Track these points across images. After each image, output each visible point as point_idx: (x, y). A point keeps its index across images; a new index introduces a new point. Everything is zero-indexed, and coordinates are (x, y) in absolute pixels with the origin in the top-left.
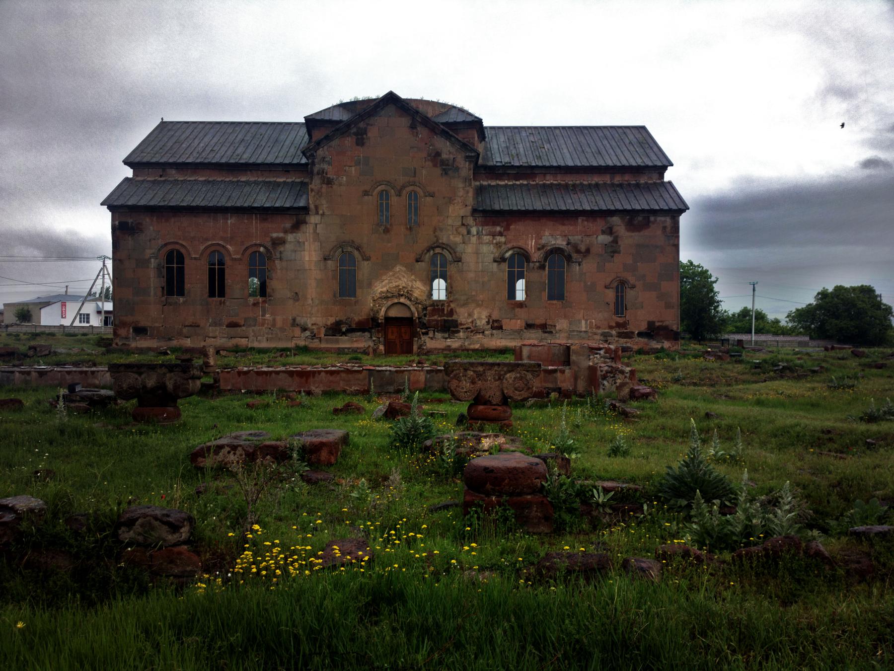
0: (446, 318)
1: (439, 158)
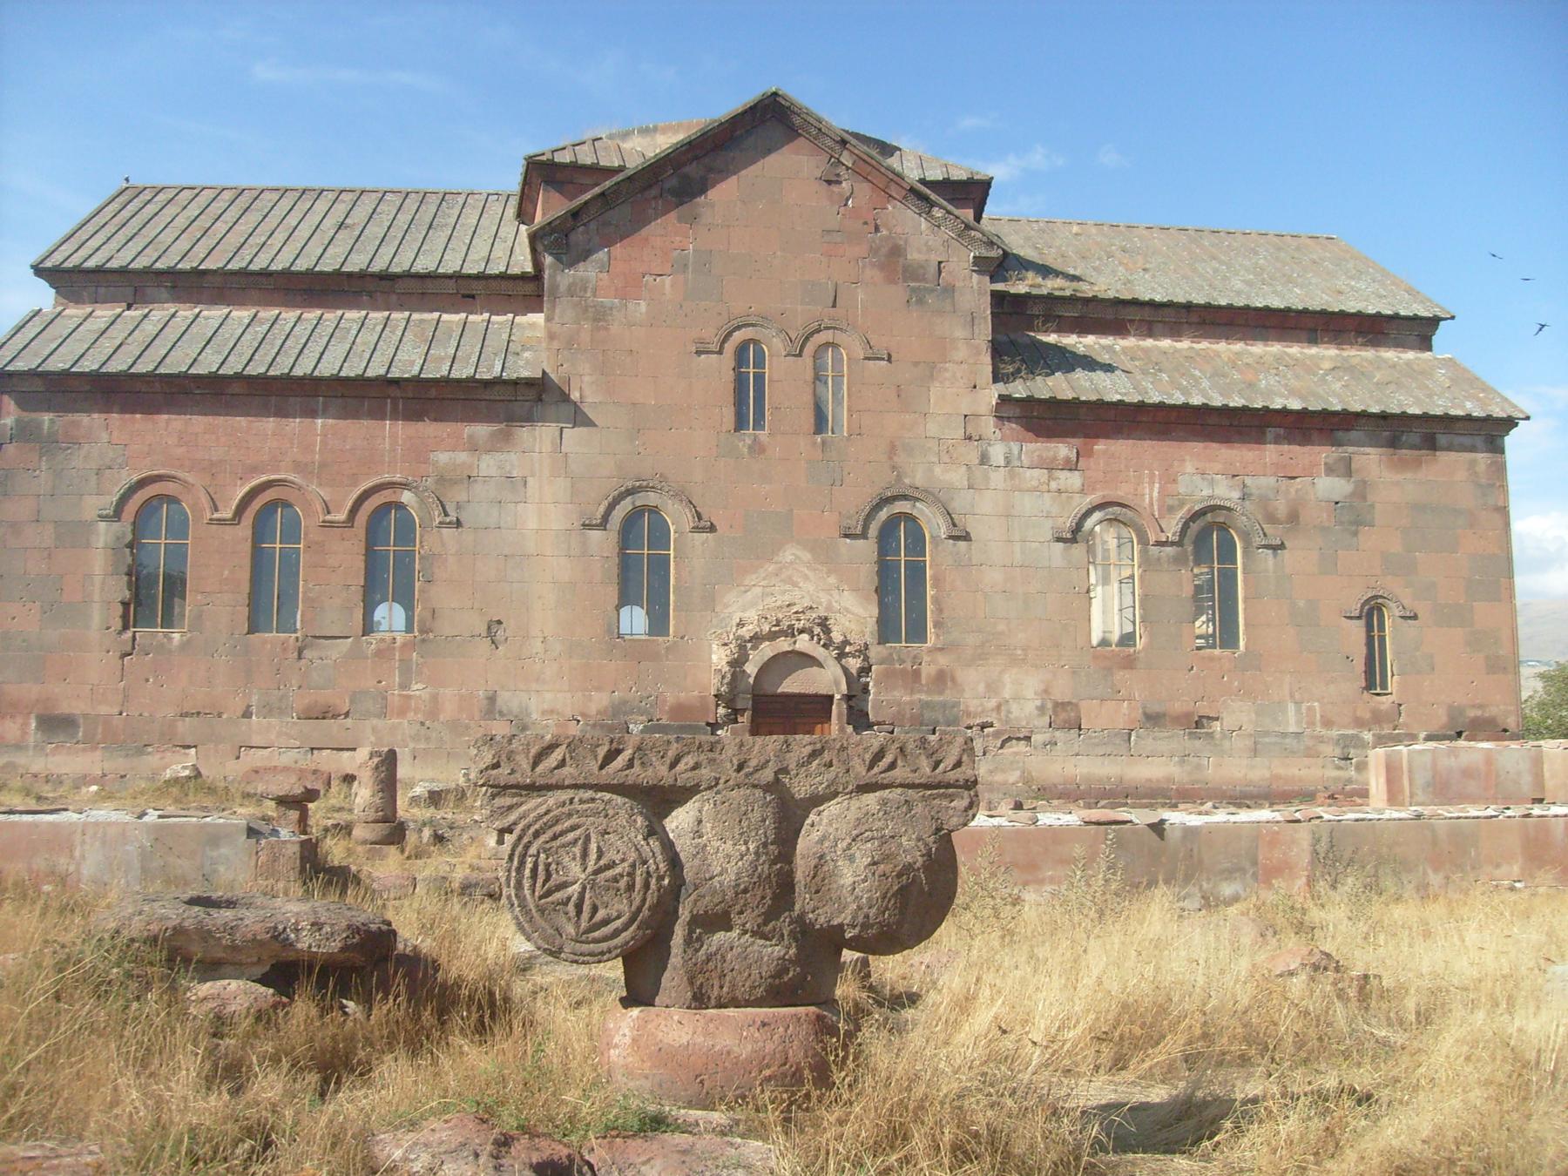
0: (923, 697)
1: (901, 260)
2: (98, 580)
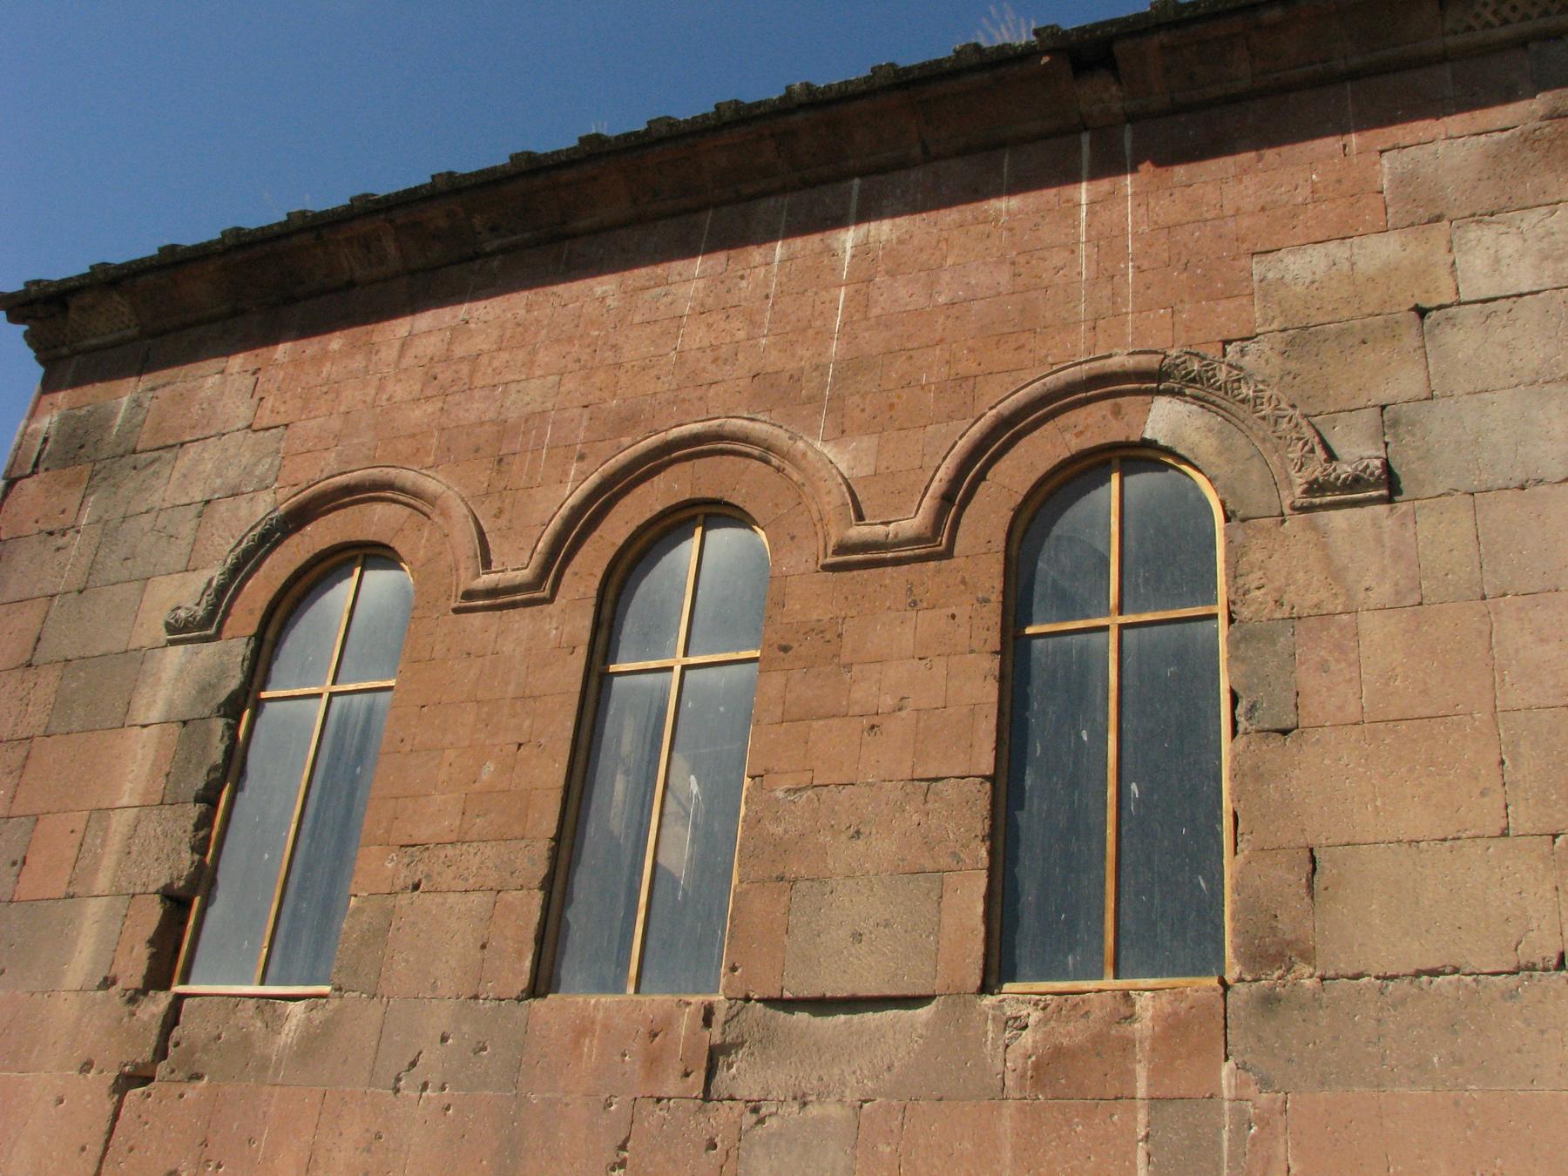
2: (120, 823)
